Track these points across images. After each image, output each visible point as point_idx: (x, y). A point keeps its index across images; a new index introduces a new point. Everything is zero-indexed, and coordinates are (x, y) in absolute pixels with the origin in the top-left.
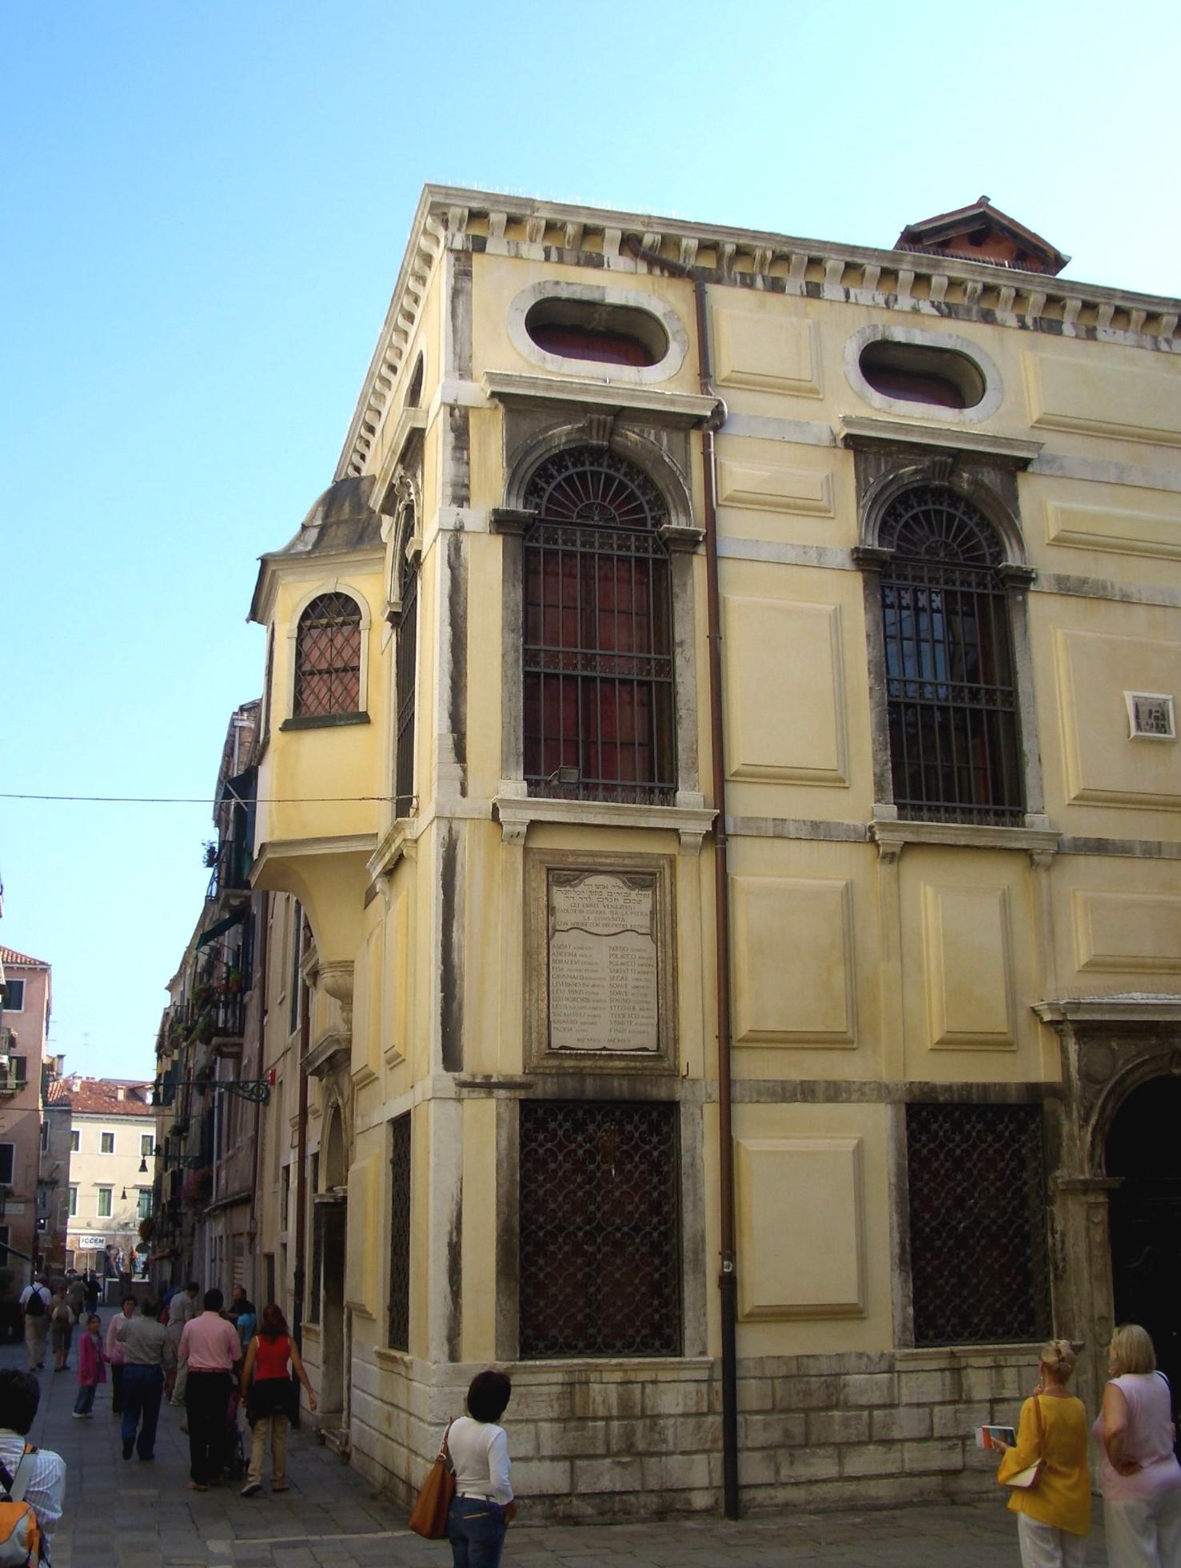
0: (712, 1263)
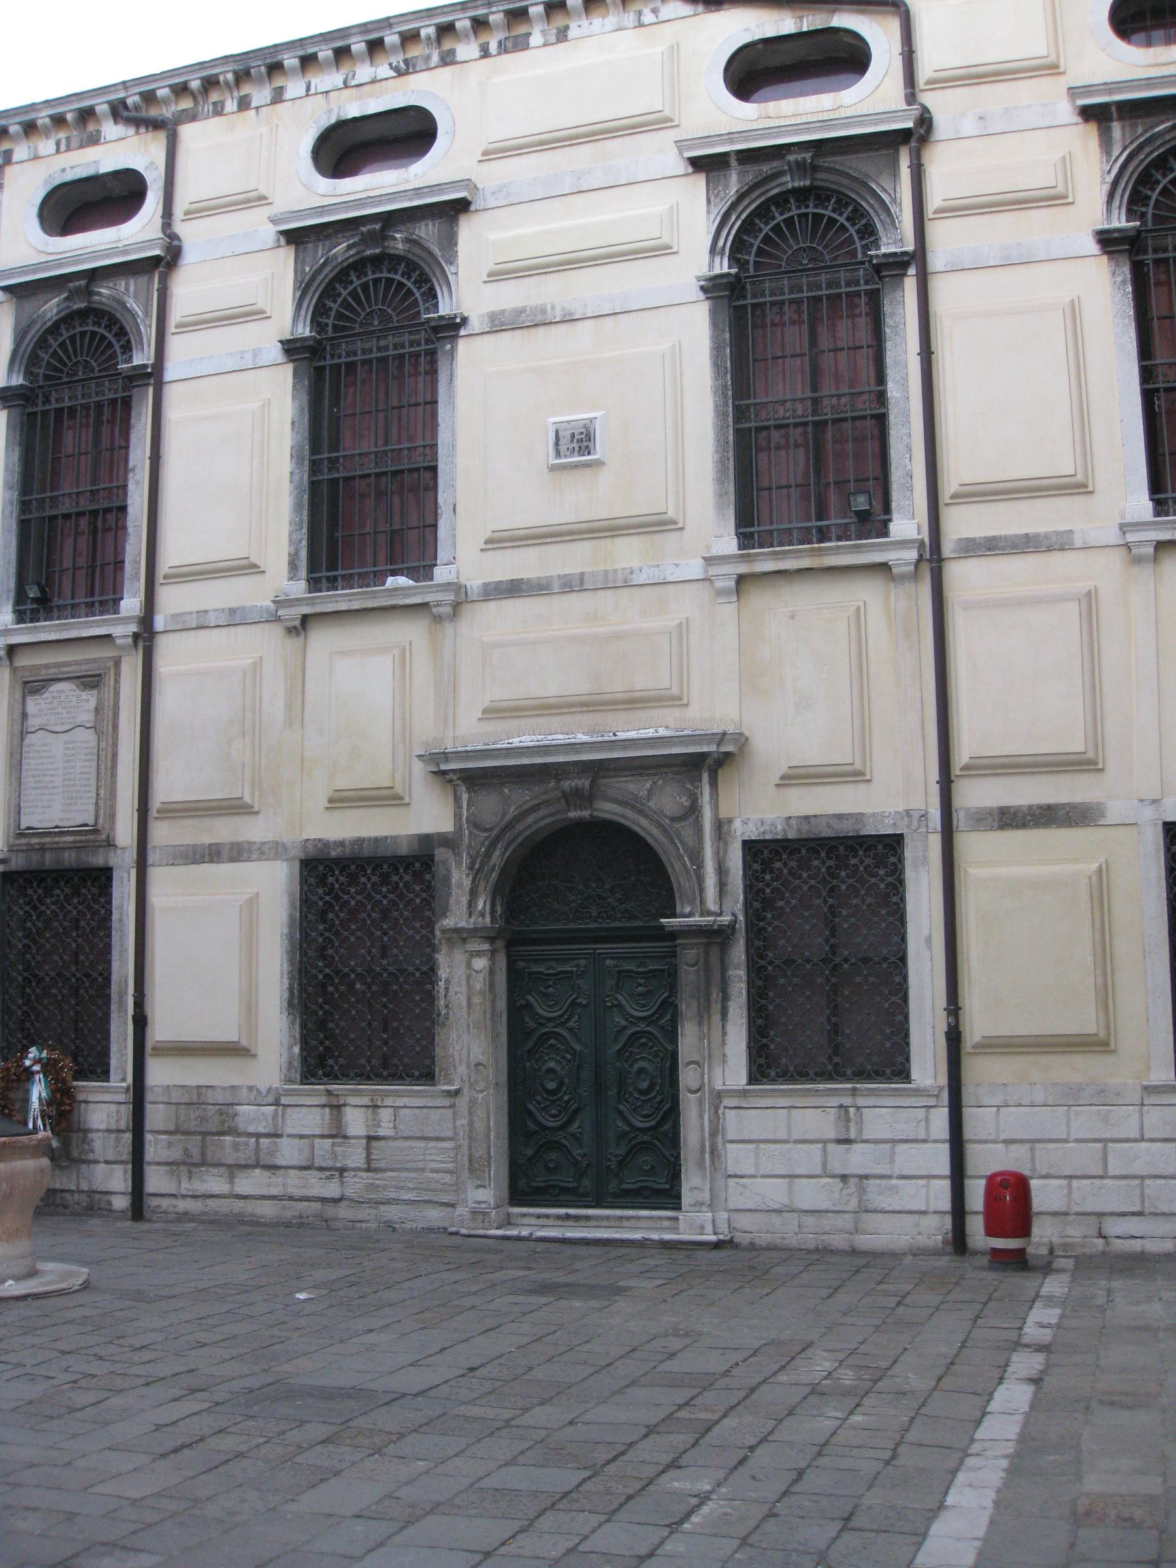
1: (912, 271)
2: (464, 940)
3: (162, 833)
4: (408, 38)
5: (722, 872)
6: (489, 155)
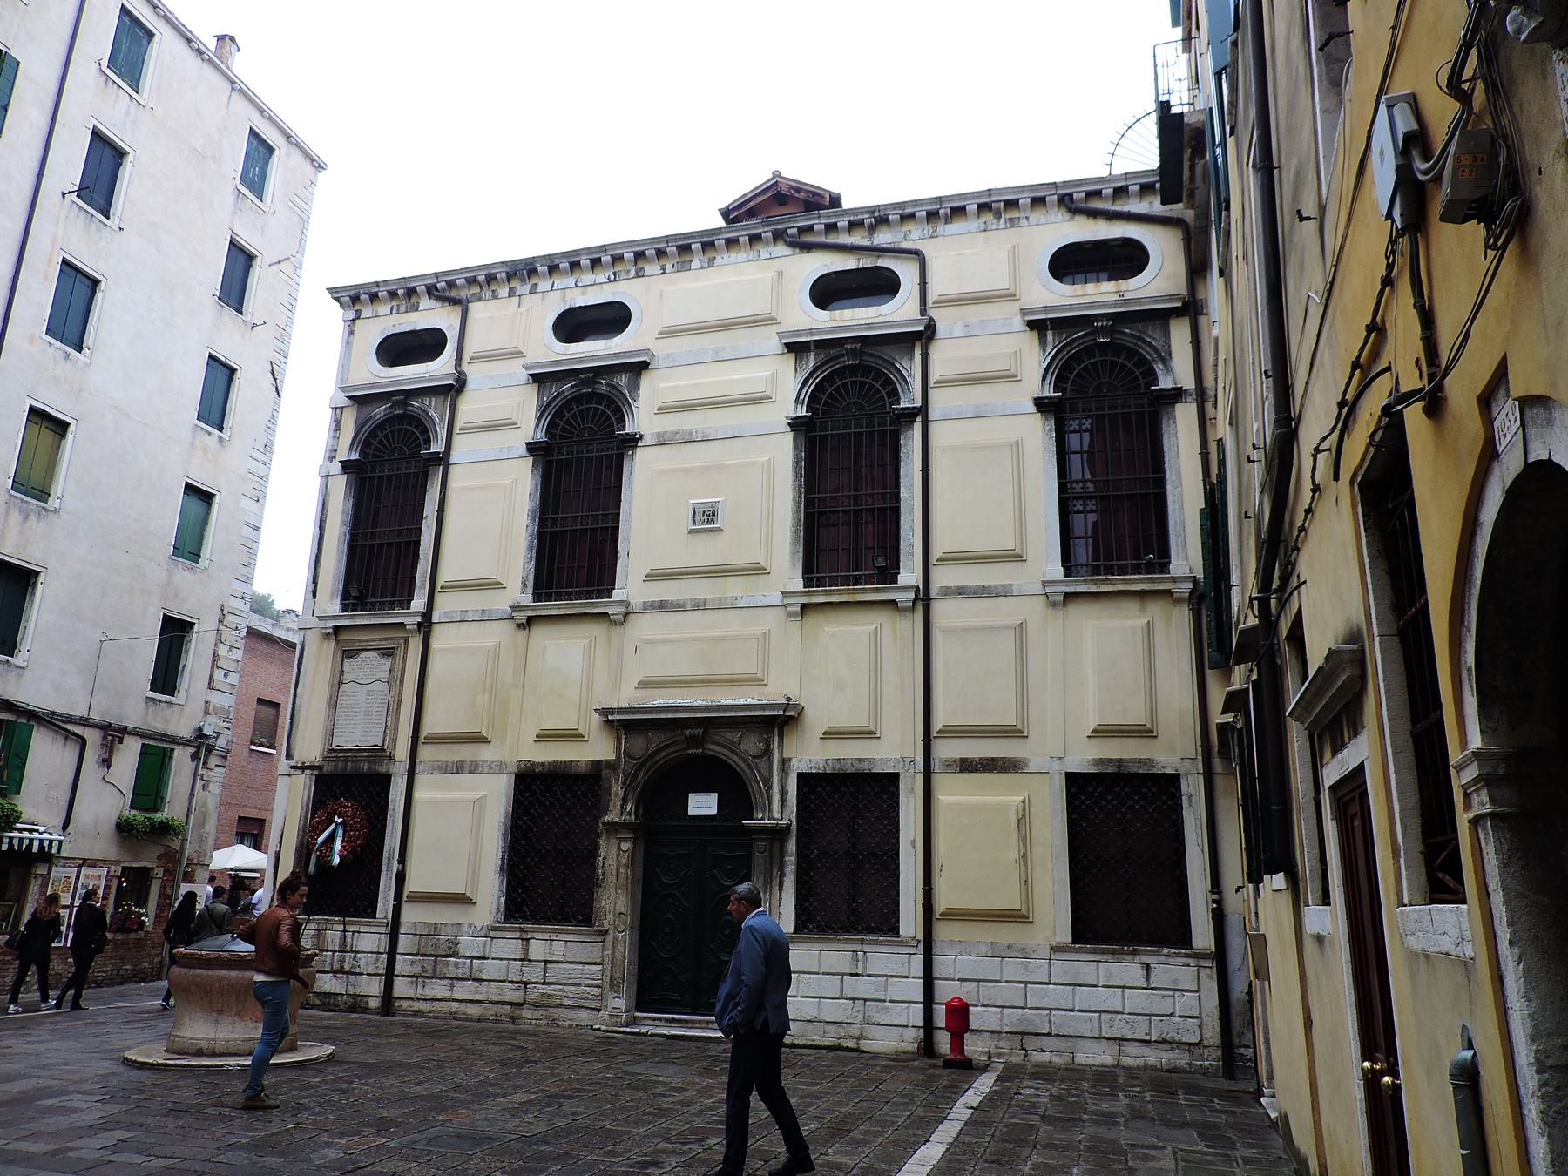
0: (395, 866)
1: (919, 419)
2: (617, 831)
3: (426, 753)
4: (617, 259)
5: (784, 792)
6: (666, 333)
